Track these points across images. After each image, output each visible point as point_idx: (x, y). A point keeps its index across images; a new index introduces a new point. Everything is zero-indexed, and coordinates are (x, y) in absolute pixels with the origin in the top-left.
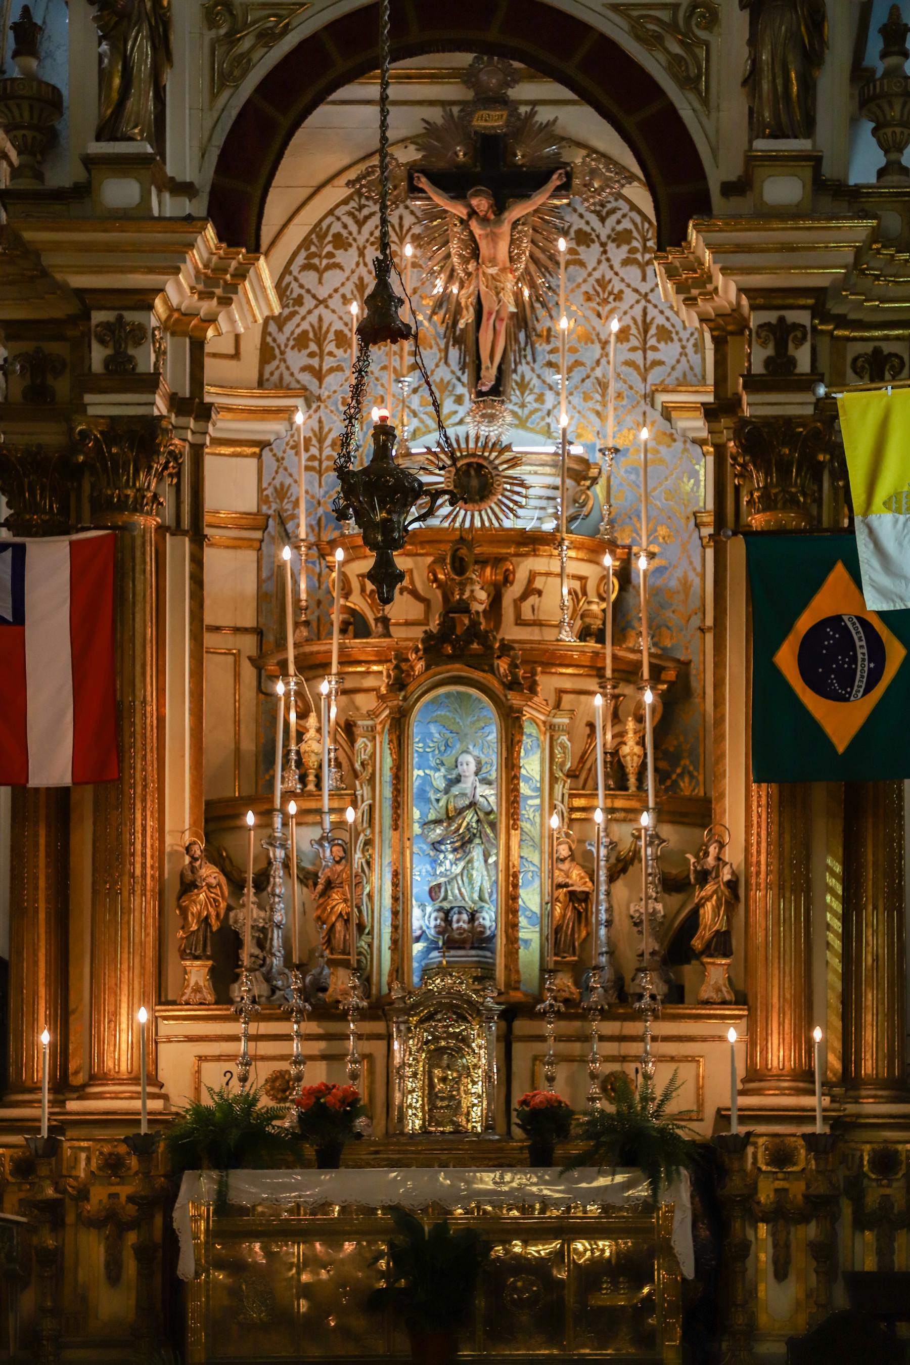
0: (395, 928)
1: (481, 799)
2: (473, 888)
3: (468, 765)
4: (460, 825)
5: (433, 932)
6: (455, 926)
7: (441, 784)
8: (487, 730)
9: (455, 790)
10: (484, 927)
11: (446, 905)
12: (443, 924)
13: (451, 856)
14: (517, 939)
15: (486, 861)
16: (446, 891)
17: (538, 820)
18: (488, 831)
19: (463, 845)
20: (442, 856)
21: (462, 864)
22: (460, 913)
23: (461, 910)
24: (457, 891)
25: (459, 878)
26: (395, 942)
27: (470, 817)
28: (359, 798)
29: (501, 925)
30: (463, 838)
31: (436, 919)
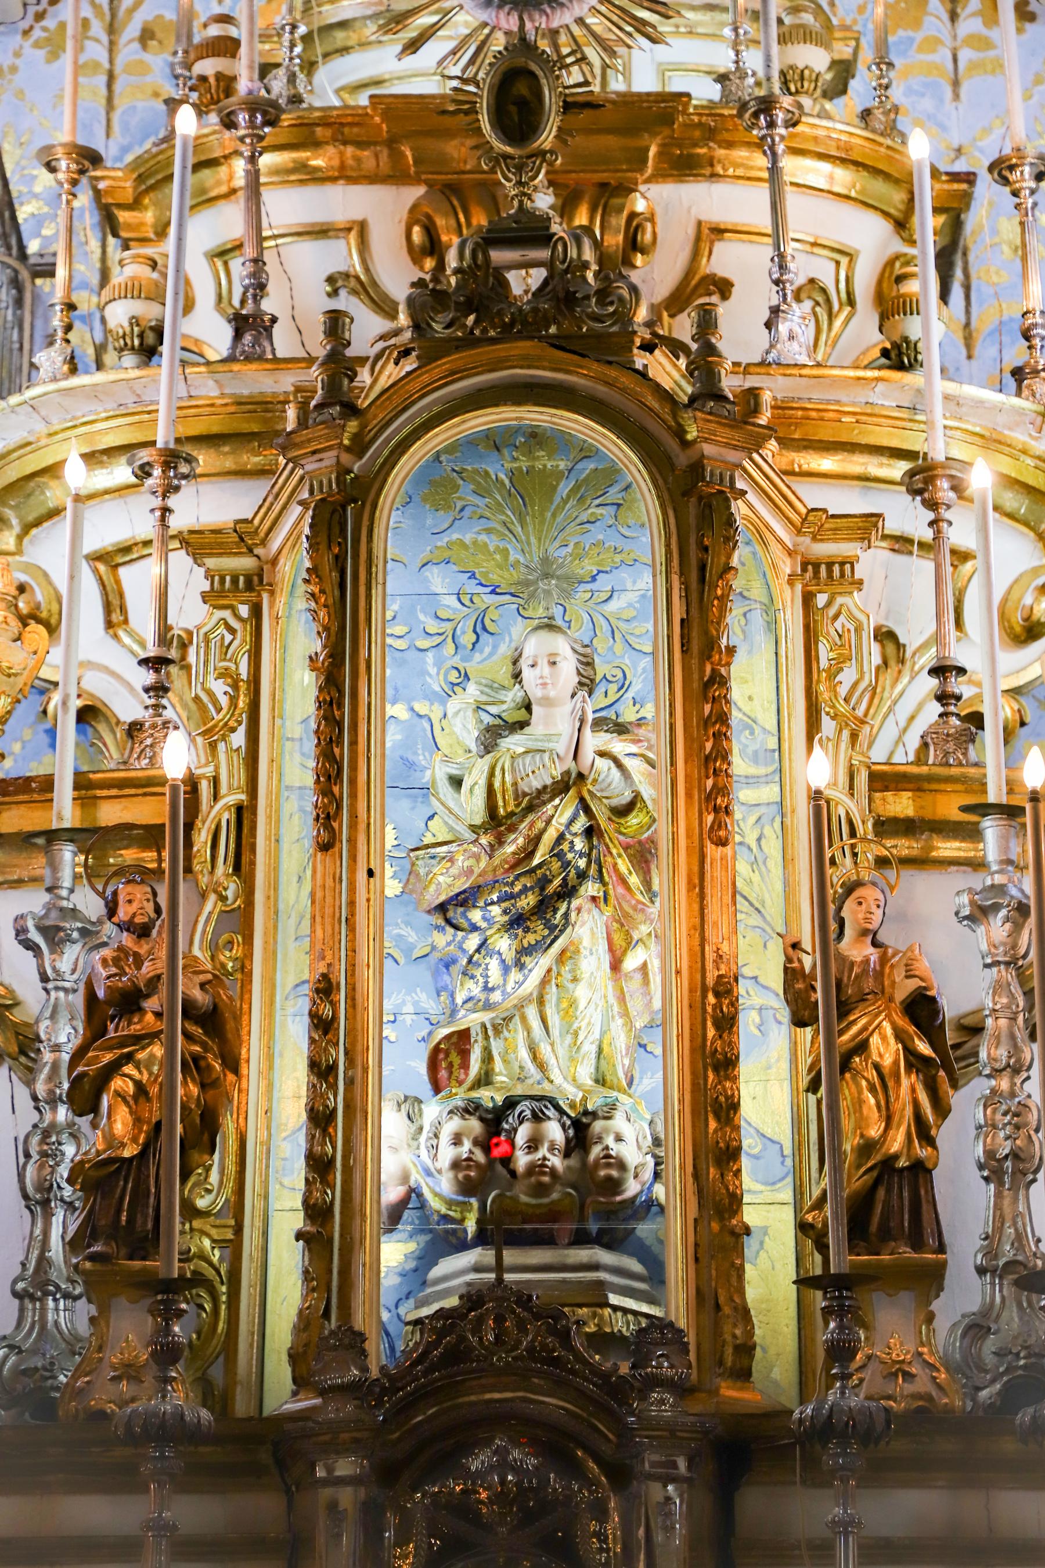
0: (319, 1166)
1: (603, 764)
2: (576, 1047)
3: (550, 668)
4: (535, 841)
5: (446, 1184)
6: (522, 1160)
7: (463, 729)
8: (604, 583)
9: (513, 743)
10: (622, 1166)
11: (487, 1097)
12: (480, 1157)
13: (504, 944)
14: (735, 1202)
15: (616, 966)
16: (488, 1058)
17: (773, 847)
18: (624, 865)
19: (541, 905)
20: (473, 941)
21: (540, 965)
22: (538, 1118)
23: (543, 1105)
24: (524, 1054)
25: (532, 1013)
26: (316, 1211)
27: (562, 813)
28: (205, 788)
29: (678, 1157)
30: (545, 881)
31: (457, 1140)
